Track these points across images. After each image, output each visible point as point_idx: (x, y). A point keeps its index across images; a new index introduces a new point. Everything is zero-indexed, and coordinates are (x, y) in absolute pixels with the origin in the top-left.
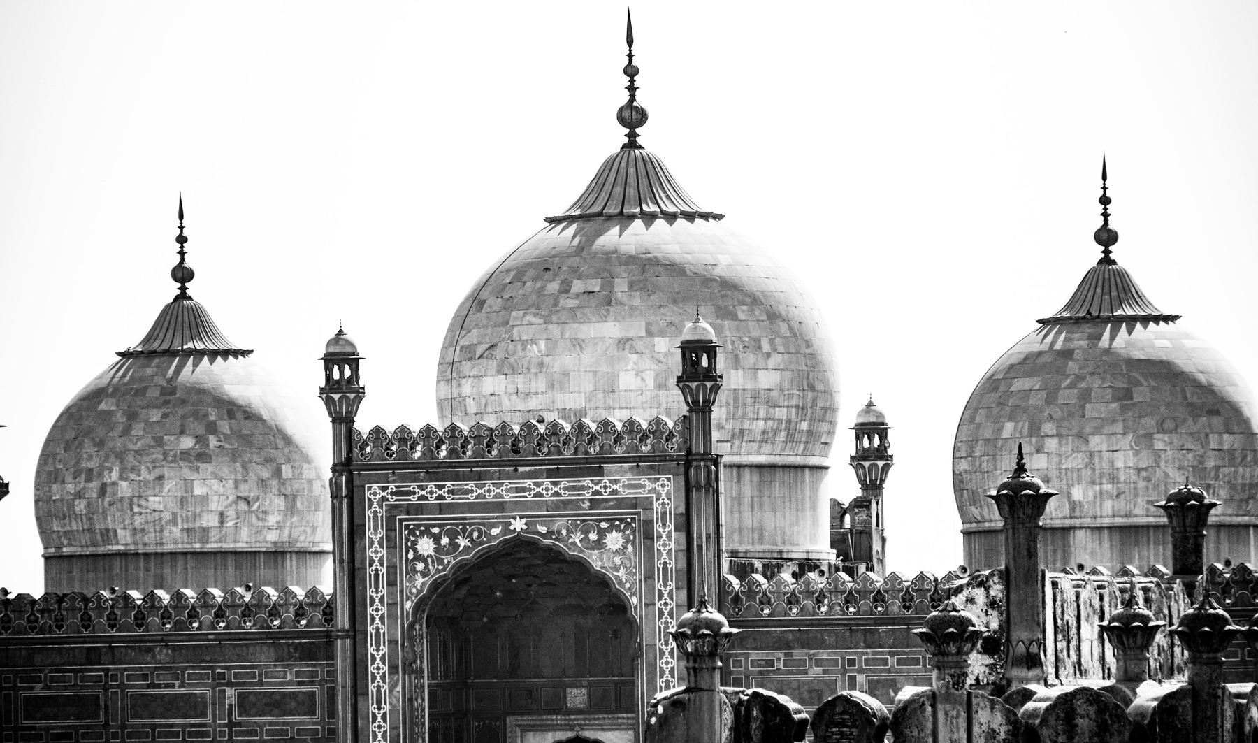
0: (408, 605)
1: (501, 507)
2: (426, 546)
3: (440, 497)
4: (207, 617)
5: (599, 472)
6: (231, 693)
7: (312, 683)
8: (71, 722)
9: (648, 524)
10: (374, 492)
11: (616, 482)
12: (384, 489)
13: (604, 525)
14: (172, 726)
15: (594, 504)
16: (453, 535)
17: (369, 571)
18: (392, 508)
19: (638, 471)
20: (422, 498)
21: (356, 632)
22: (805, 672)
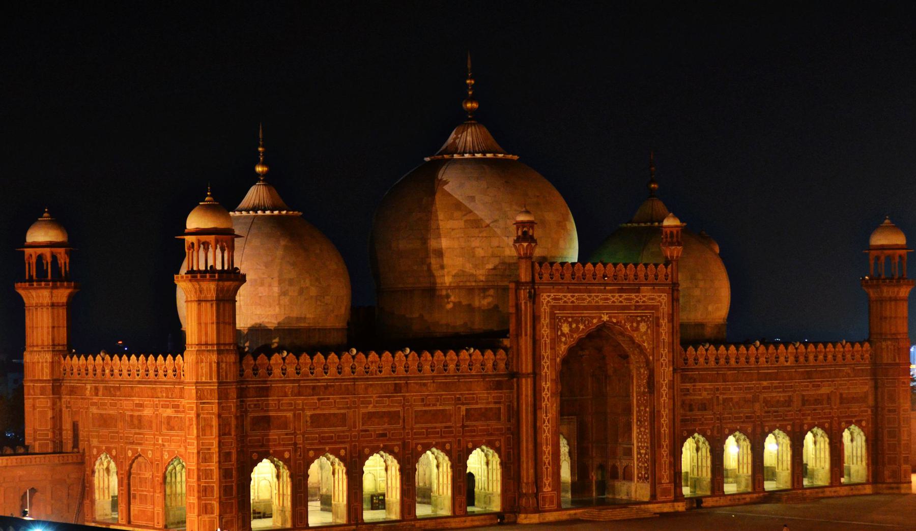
0: (558, 360)
1: (598, 308)
2: (566, 329)
3: (573, 302)
4: (452, 366)
5: (638, 291)
6: (463, 408)
7: (499, 403)
8: (386, 426)
9: (658, 318)
10: (546, 299)
11: (644, 296)
12: (549, 296)
13: (639, 319)
14: (435, 428)
15: (637, 307)
16: (577, 323)
17: (543, 341)
18: (553, 307)
19: (654, 290)
20: (565, 302)
21: (536, 375)
22: (700, 395)
